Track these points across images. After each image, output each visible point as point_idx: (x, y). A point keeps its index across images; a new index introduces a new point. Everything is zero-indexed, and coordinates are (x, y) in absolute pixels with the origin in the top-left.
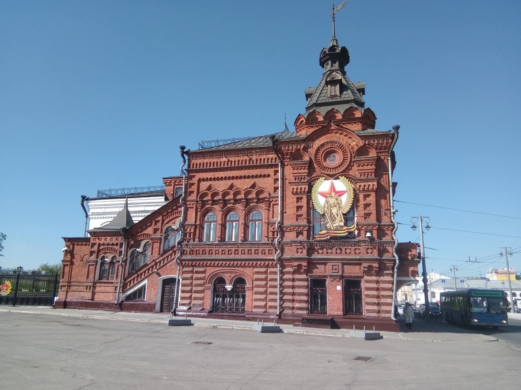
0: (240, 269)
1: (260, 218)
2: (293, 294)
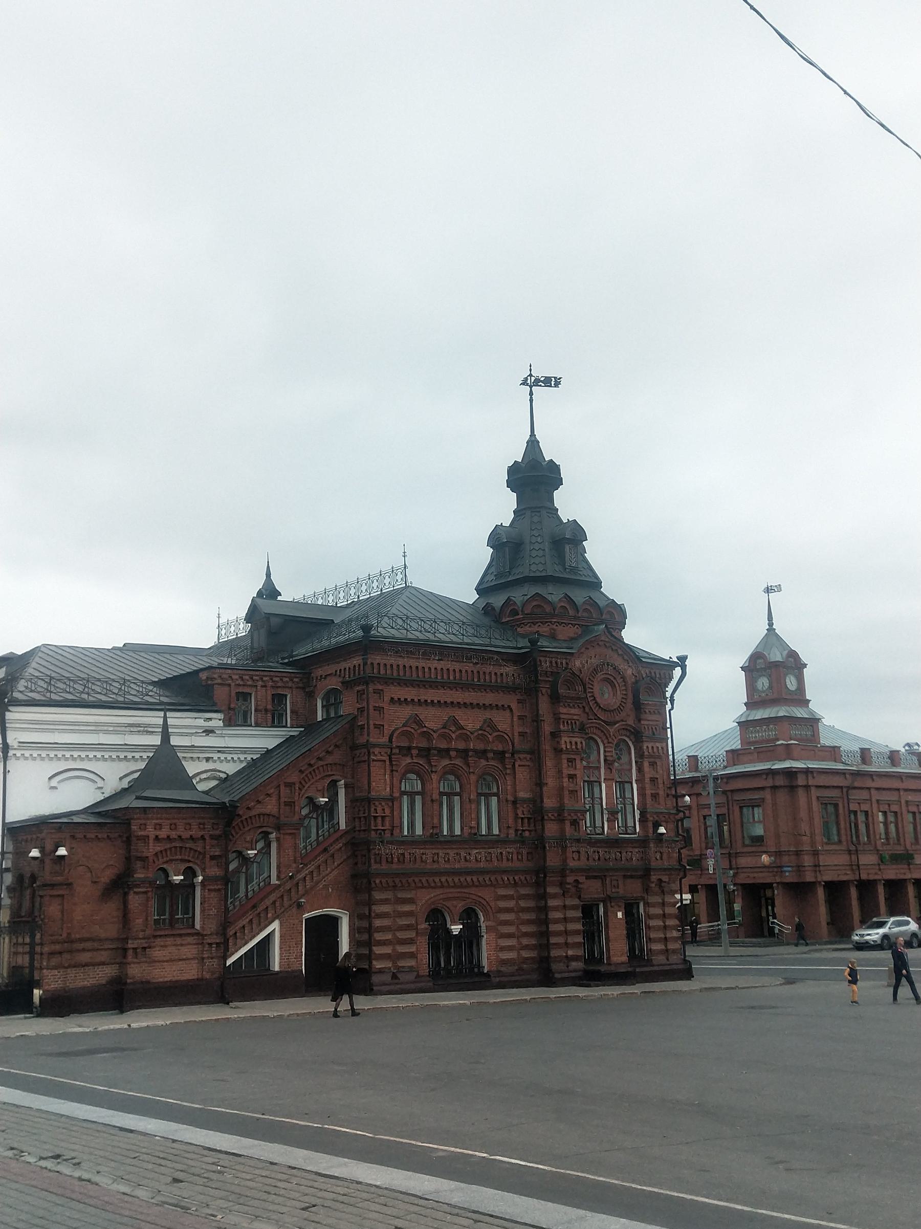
0: (473, 890)
1: (495, 790)
2: (566, 933)
